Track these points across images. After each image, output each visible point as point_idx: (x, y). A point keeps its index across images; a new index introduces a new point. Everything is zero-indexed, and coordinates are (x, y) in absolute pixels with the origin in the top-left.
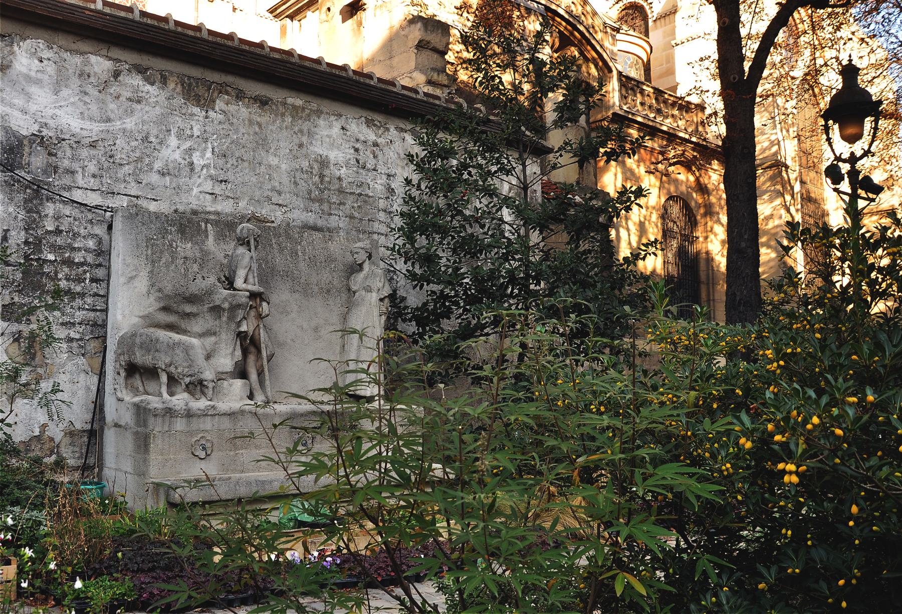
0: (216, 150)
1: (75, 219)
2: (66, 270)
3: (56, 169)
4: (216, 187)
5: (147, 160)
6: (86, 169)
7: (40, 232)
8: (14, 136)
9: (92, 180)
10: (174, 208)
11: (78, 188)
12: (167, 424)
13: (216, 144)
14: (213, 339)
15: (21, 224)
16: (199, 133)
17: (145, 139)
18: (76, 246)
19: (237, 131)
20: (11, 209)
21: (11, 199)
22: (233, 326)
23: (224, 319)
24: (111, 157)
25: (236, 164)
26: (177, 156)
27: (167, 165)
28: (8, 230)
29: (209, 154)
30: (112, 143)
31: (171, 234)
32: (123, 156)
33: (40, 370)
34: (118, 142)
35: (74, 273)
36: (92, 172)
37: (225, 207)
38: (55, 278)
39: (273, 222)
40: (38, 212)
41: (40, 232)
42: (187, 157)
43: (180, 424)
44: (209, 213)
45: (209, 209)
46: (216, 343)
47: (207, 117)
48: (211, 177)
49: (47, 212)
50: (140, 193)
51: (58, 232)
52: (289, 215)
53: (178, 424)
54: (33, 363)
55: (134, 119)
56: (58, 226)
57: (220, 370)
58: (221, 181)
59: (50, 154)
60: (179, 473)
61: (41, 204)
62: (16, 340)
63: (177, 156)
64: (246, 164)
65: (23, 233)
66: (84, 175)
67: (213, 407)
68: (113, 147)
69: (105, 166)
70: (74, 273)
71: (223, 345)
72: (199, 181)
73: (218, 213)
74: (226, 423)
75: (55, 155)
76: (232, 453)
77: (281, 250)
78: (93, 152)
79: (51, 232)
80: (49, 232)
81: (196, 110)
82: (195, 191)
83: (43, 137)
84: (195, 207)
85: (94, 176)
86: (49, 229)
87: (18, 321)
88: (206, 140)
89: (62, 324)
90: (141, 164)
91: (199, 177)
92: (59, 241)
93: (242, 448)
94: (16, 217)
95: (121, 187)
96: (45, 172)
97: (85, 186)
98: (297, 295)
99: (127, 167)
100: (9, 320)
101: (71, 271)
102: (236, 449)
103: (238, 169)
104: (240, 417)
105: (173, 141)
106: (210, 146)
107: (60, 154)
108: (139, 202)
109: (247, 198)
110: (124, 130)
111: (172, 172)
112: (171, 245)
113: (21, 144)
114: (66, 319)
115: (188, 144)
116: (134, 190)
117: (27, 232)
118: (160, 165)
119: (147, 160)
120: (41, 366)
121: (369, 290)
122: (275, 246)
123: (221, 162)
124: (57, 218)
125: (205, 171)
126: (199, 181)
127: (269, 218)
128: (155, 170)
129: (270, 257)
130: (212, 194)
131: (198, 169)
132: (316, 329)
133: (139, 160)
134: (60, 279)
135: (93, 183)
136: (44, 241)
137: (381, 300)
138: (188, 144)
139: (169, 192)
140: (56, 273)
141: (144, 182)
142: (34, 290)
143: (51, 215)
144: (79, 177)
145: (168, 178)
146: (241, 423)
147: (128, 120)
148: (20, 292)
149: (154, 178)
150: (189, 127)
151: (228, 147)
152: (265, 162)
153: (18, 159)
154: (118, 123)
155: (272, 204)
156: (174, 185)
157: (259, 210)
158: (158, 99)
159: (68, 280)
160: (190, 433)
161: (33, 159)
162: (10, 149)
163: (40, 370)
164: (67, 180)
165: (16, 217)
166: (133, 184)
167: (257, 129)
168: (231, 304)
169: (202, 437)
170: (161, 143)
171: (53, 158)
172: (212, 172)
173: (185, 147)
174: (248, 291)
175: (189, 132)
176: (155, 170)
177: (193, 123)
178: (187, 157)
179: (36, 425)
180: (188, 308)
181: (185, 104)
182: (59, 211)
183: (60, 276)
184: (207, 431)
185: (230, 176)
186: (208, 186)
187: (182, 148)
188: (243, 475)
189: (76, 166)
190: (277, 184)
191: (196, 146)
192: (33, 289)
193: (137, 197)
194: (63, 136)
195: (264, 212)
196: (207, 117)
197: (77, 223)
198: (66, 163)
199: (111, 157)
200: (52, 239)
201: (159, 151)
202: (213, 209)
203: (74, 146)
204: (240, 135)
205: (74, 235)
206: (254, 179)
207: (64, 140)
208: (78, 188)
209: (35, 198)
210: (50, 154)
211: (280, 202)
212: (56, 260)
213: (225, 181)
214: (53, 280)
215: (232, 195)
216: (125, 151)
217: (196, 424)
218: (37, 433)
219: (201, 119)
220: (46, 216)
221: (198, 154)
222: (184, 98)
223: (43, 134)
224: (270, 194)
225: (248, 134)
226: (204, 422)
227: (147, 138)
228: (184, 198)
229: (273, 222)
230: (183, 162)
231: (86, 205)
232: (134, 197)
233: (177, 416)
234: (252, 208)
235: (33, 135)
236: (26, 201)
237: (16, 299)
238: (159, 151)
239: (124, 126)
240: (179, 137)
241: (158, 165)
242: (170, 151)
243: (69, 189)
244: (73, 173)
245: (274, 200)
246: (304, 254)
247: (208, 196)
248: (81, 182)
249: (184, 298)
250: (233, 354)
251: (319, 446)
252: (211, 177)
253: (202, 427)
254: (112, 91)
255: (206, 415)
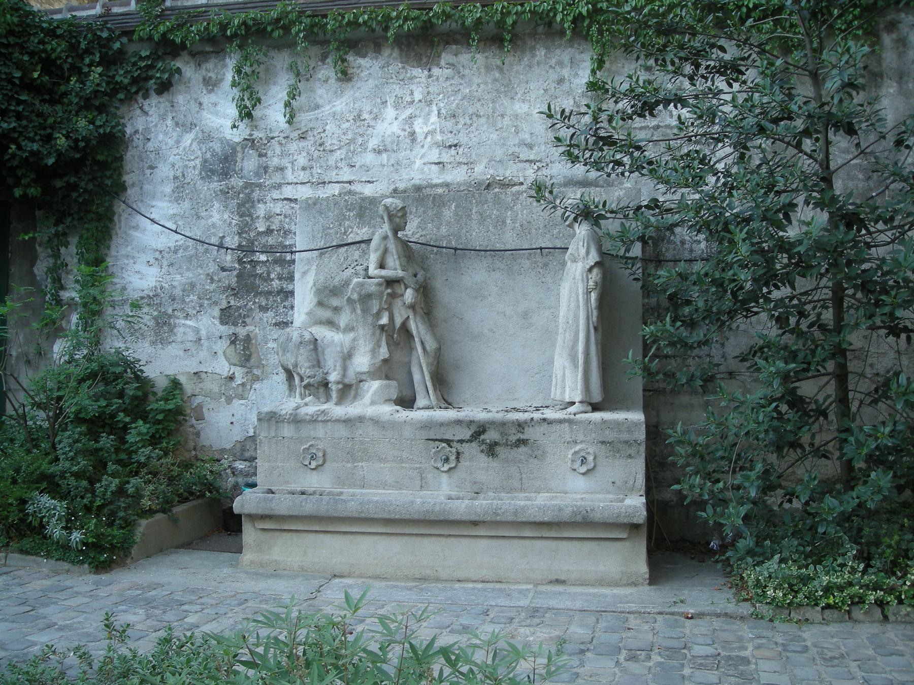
0: (443, 111)
1: (285, 217)
2: (278, 269)
3: (266, 169)
4: (444, 154)
5: (360, 140)
6: (295, 163)
7: (252, 234)
8: (229, 145)
9: (302, 173)
10: (393, 187)
11: (288, 184)
12: (274, 428)
13: (442, 105)
14: (351, 335)
15: (235, 229)
16: (421, 97)
17: (358, 118)
18: (287, 243)
19: (469, 84)
20: (226, 216)
21: (226, 207)
22: (370, 319)
23: (359, 312)
24: (320, 145)
25: (469, 122)
26: (395, 128)
27: (383, 141)
28: (224, 237)
29: (434, 118)
30: (321, 130)
31: (349, 219)
32: (335, 142)
33: (255, 371)
34: (328, 128)
35: (285, 271)
36: (302, 165)
37: (457, 176)
38: (268, 279)
39: (522, 184)
40: (250, 215)
41: (252, 234)
42: (407, 127)
43: (287, 431)
44: (436, 186)
45: (436, 181)
46: (354, 340)
47: (430, 76)
48: (437, 145)
49: (258, 213)
50: (353, 178)
51: (269, 232)
52: (545, 172)
53: (286, 430)
54: (248, 365)
55: (344, 99)
56: (269, 226)
57: (358, 370)
58: (450, 147)
59: (260, 155)
60: (288, 483)
61: (253, 207)
62: (233, 343)
63: (395, 128)
64: (483, 120)
65: (237, 237)
66: (293, 170)
67: (323, 412)
68: (322, 135)
69: (315, 156)
70: (285, 271)
71: (361, 342)
72: (423, 151)
73: (447, 185)
74: (342, 431)
75: (265, 155)
76: (349, 465)
77: (483, 219)
78: (303, 144)
79: (263, 233)
80: (260, 234)
81: (417, 72)
82: (418, 163)
83: (253, 140)
84: (418, 182)
85: (304, 169)
86: (261, 229)
87: (235, 324)
88: (430, 103)
89: (276, 324)
90: (354, 145)
91: (423, 146)
92: (271, 240)
93: (362, 460)
94: (230, 223)
95: (332, 175)
96: (257, 174)
97: (295, 180)
98: (497, 275)
99: (339, 152)
100: (227, 323)
101: (282, 270)
102: (354, 461)
103: (473, 128)
104: (358, 424)
105: (390, 113)
106: (434, 108)
107: (270, 153)
108: (353, 187)
109: (485, 161)
110: (334, 113)
111: (389, 147)
112: (345, 232)
113: (234, 151)
114: (279, 319)
115: (408, 112)
116: (346, 174)
117: (240, 237)
118: (376, 142)
119: (360, 140)
120: (258, 367)
121: (574, 261)
122: (474, 216)
123: (449, 124)
124: (268, 217)
125: (429, 138)
126: (423, 151)
127: (516, 180)
128: (370, 148)
129: (464, 231)
130: (439, 163)
131: (420, 138)
132: (525, 315)
133: (352, 141)
134: (272, 280)
135: (303, 176)
136: (256, 243)
137: (590, 270)
138: (408, 112)
139: (386, 170)
140: (269, 274)
141: (358, 165)
142: (248, 292)
143: (262, 215)
144: (289, 172)
145: (385, 156)
146: (360, 432)
147: (338, 102)
148: (235, 295)
149: (369, 158)
150: (409, 92)
151: (458, 105)
152: (509, 112)
153: (232, 167)
154: (328, 107)
155: (520, 161)
156: (392, 161)
157: (501, 172)
158: (371, 71)
159: (280, 278)
160: (301, 440)
161: (245, 163)
162: (225, 158)
163: (255, 371)
164: (277, 178)
165: (230, 223)
166: (346, 169)
167: (497, 75)
168: (359, 294)
169: (311, 446)
170: (375, 118)
171: (264, 159)
172: (439, 137)
173: (404, 117)
174: (382, 277)
175: (408, 99)
176: (370, 148)
177: (413, 87)
178: (407, 127)
179: (250, 426)
180: (335, 302)
181: (403, 68)
182: (270, 211)
183: (272, 276)
184: (319, 439)
185: (462, 138)
186: (434, 156)
187: (400, 119)
188: (364, 491)
189: (285, 162)
190: (527, 136)
191: (417, 113)
192: (247, 291)
193: (350, 182)
194: (271, 135)
195: (508, 173)
196: (430, 76)
197: (287, 220)
198: (276, 161)
199: (320, 145)
200: (263, 240)
201: (373, 127)
202: (440, 181)
203: (283, 142)
204: (474, 87)
205: (285, 233)
206: (494, 136)
207: (273, 138)
208: (288, 184)
209: (248, 202)
210: (260, 155)
211: (532, 157)
212: (268, 260)
213: (455, 146)
214: (266, 280)
215: (465, 161)
216: (336, 135)
217: (306, 431)
218: (251, 434)
219: (423, 80)
220: (258, 217)
221: (420, 120)
222: (402, 62)
223: (254, 137)
224: (517, 149)
225: (486, 83)
226: (315, 429)
227: (359, 116)
228: (405, 174)
229: (522, 184)
230: (402, 134)
231: (296, 200)
232: (347, 182)
233: (283, 421)
234: (491, 172)
235: (245, 139)
236: (239, 206)
237: (232, 303)
238: (373, 127)
239: (334, 109)
240: (396, 107)
241: (373, 143)
242: (386, 124)
243: (279, 186)
244: (282, 169)
245: (523, 157)
246: (513, 221)
247: (434, 167)
248: (290, 177)
249: (330, 291)
250: (374, 352)
251: (468, 463)
252: (437, 145)
253: (312, 433)
254: (320, 76)
255: (316, 421)
